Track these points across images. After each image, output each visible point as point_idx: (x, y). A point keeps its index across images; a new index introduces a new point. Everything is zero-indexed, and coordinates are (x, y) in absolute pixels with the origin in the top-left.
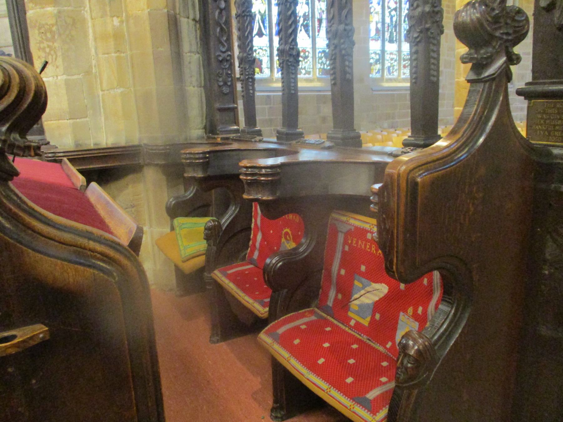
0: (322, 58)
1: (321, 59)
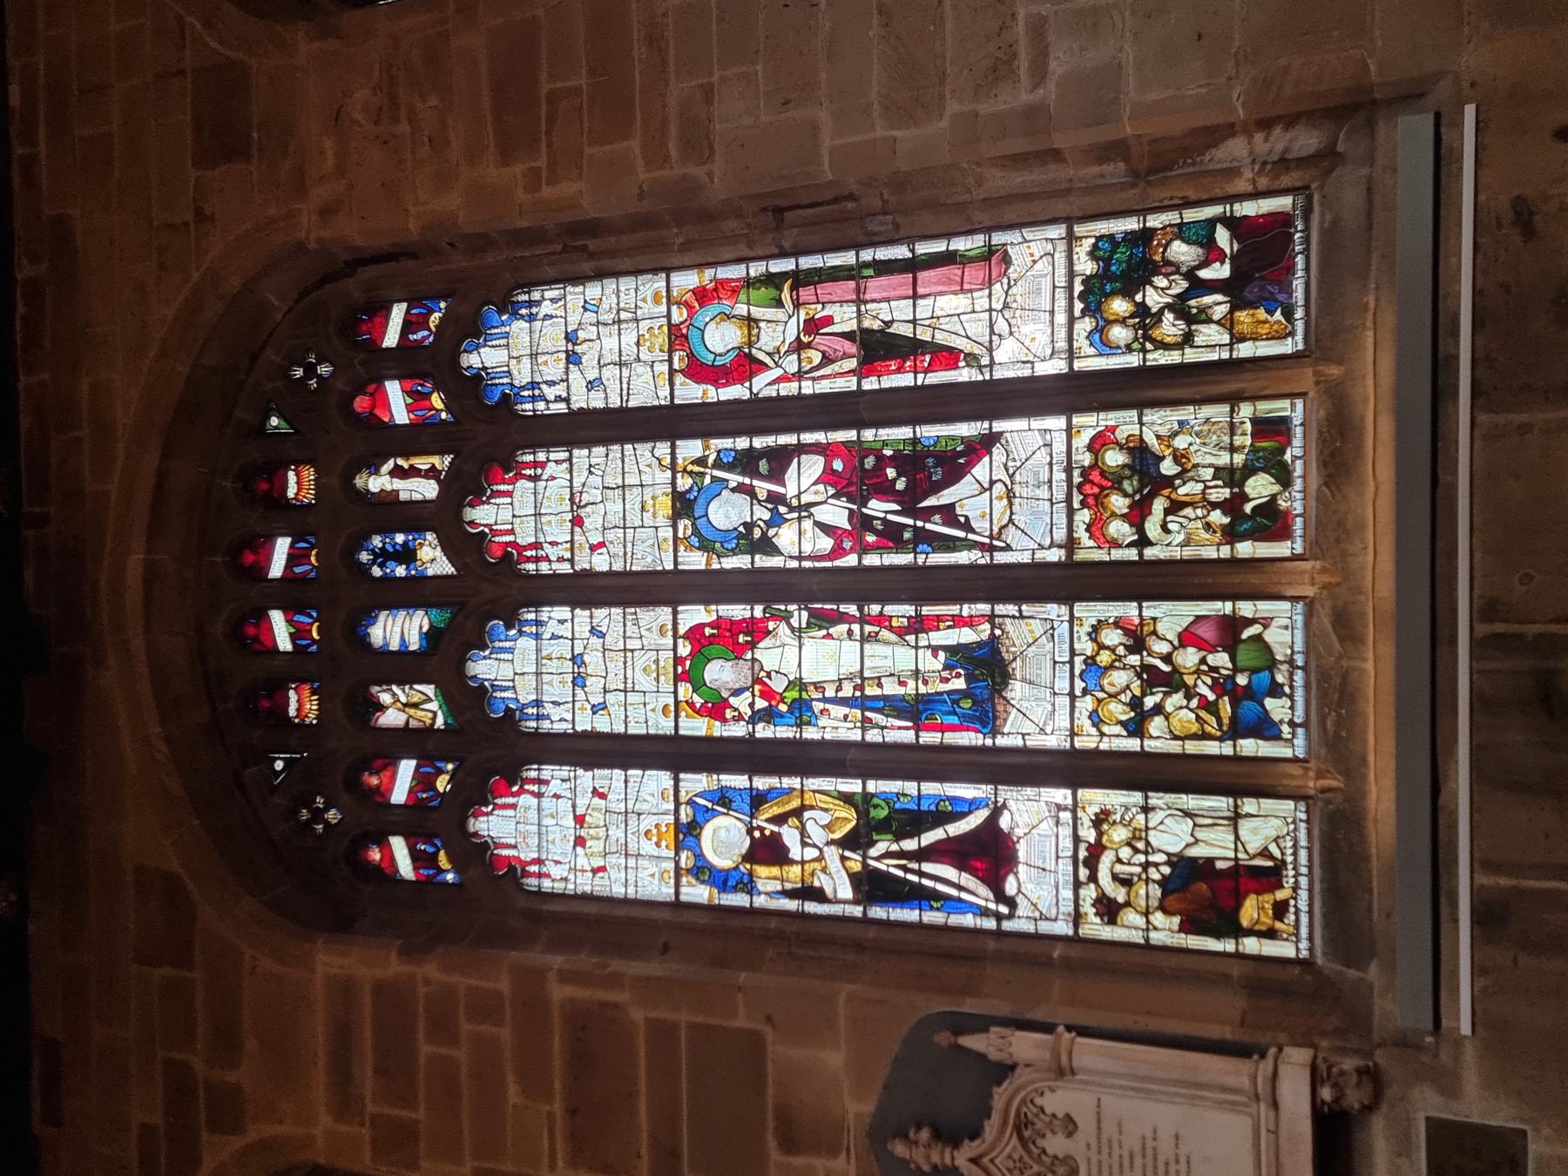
0: (1142, 310)
1: (1159, 315)
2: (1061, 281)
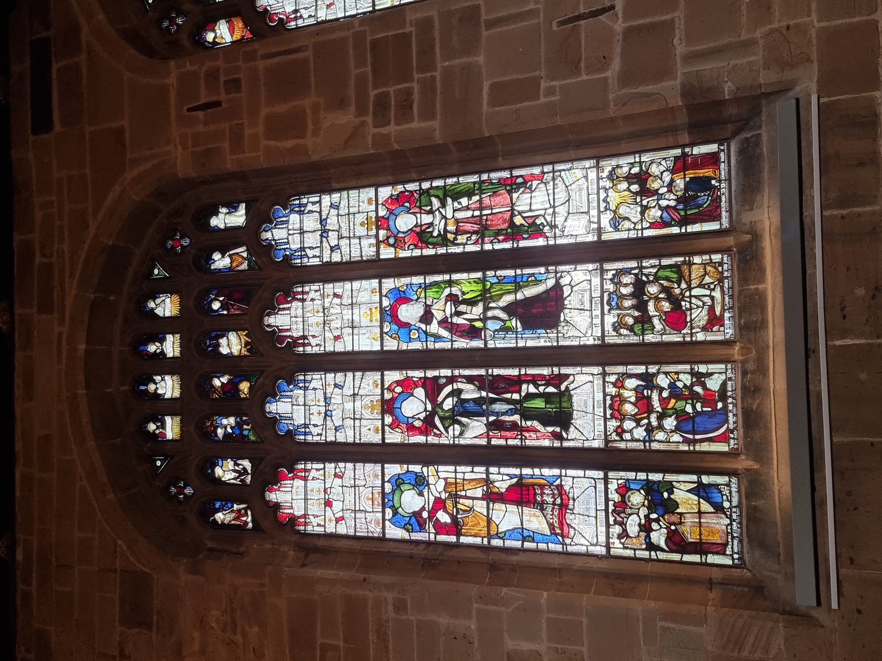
2: (602, 506)
